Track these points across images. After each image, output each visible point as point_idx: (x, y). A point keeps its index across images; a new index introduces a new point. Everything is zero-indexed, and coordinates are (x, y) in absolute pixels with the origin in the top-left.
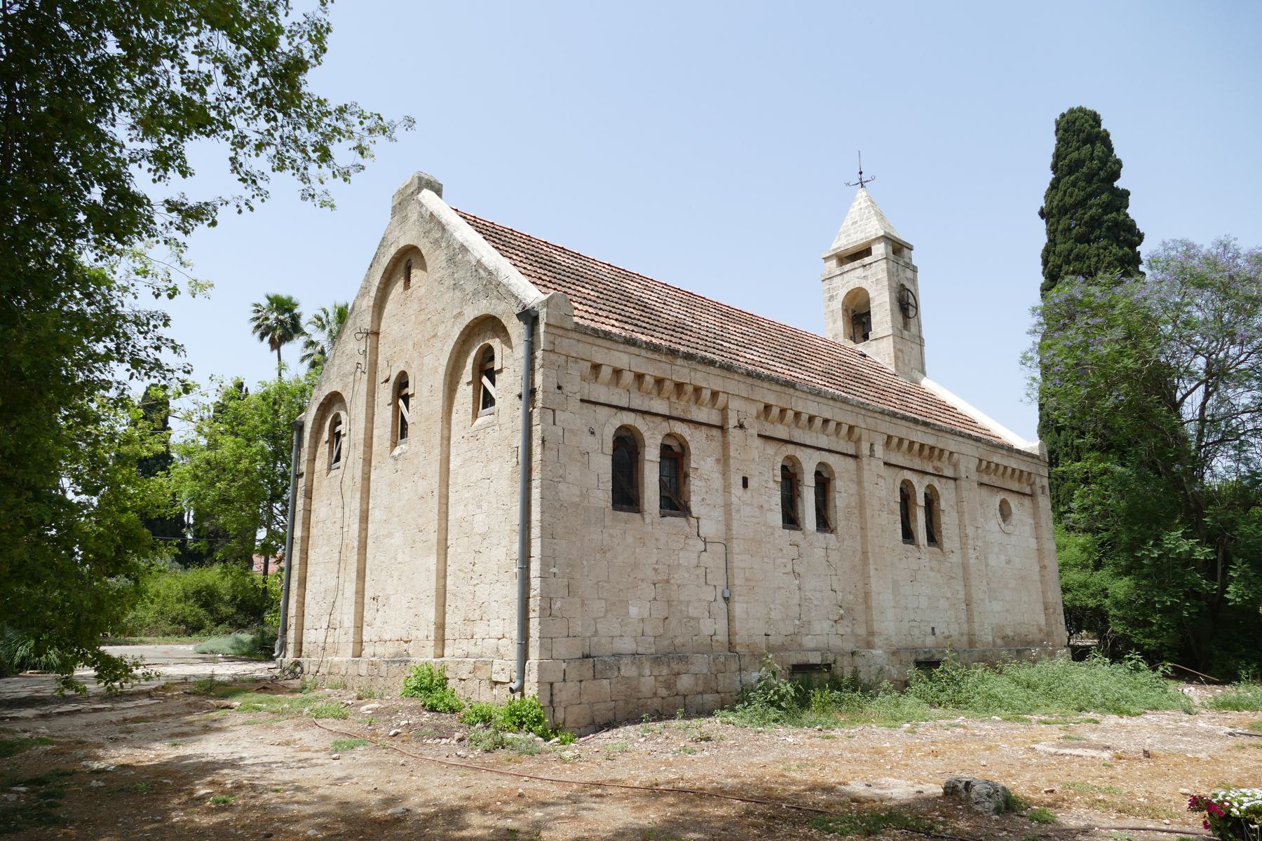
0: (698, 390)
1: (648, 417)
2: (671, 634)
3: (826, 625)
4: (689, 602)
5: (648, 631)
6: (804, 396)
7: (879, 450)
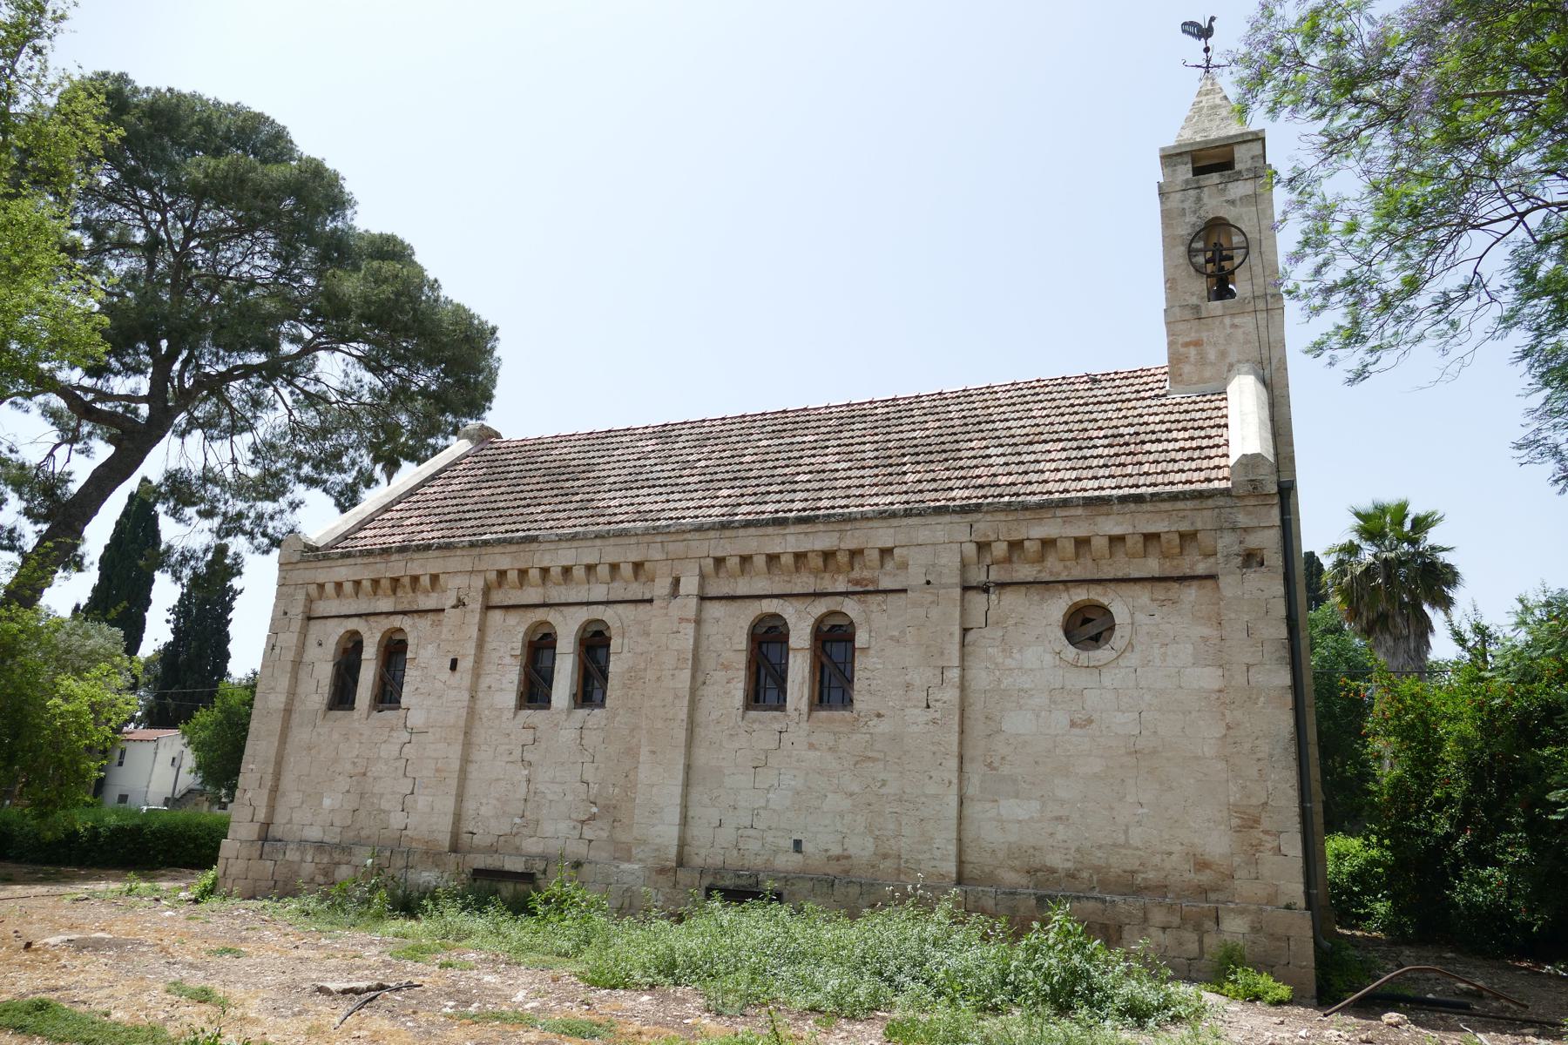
0: (415, 579)
1: (372, 619)
2: (358, 826)
3: (563, 827)
4: (382, 795)
5: (337, 823)
6: (552, 546)
7: (690, 585)
